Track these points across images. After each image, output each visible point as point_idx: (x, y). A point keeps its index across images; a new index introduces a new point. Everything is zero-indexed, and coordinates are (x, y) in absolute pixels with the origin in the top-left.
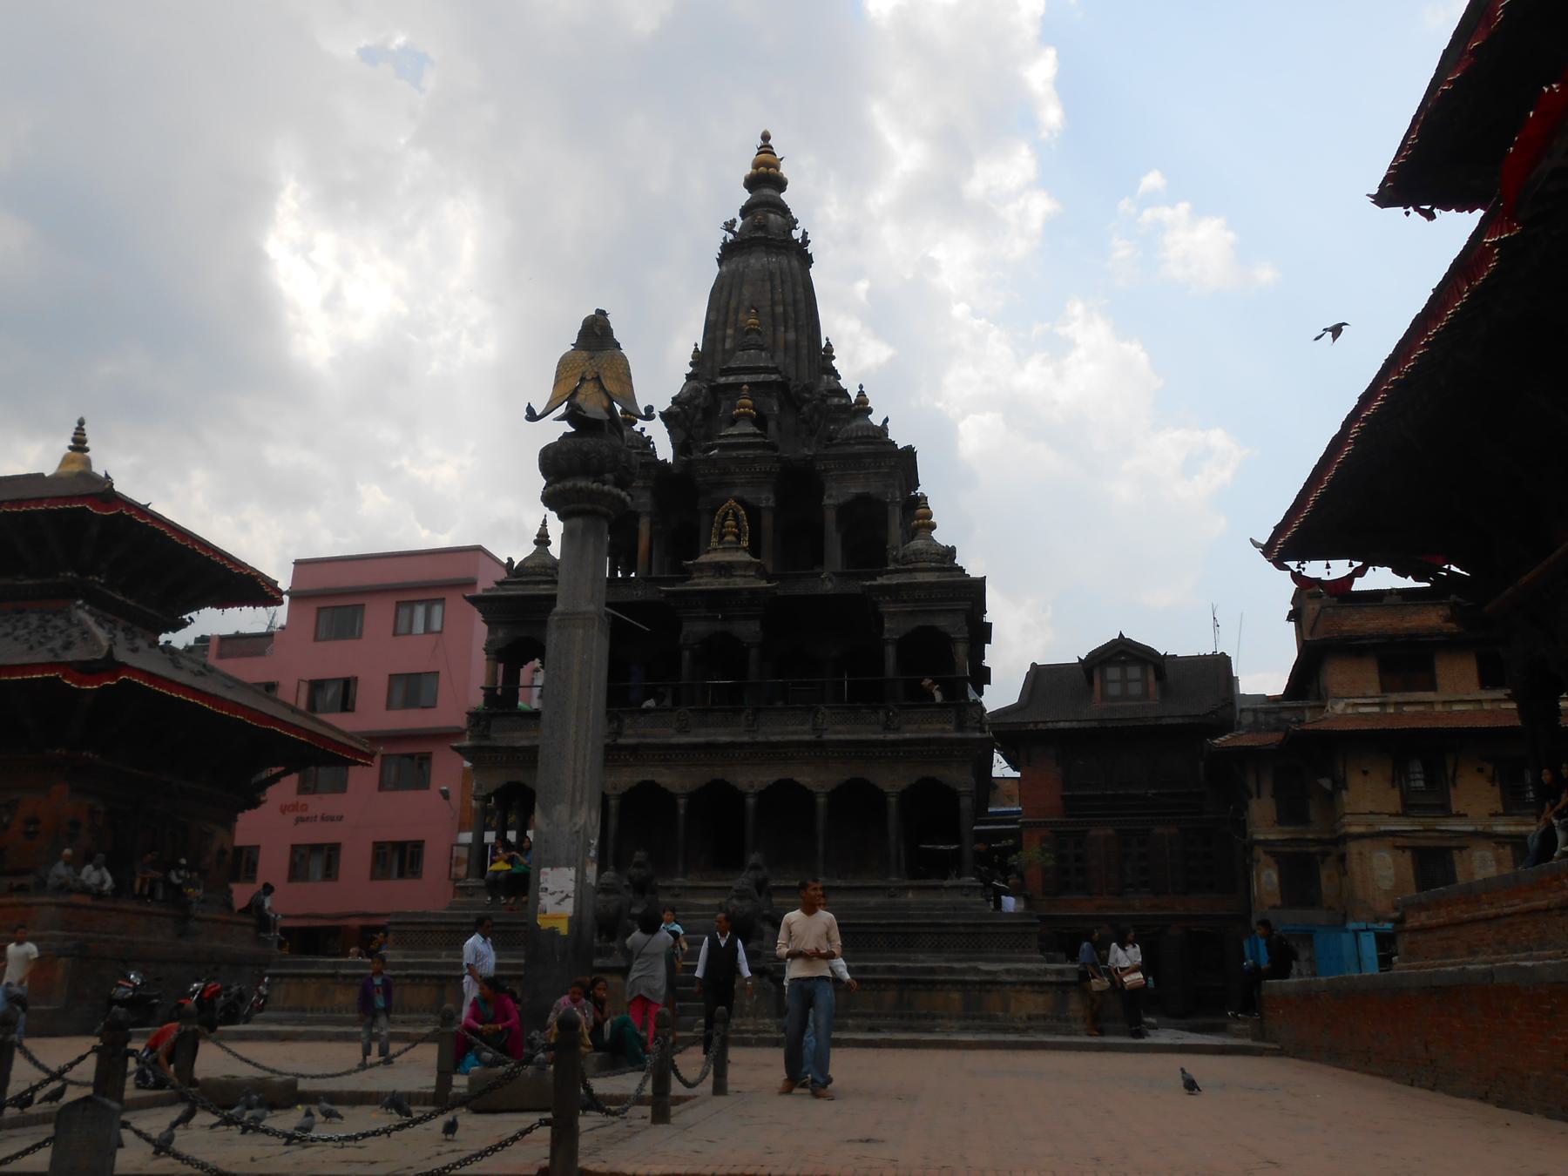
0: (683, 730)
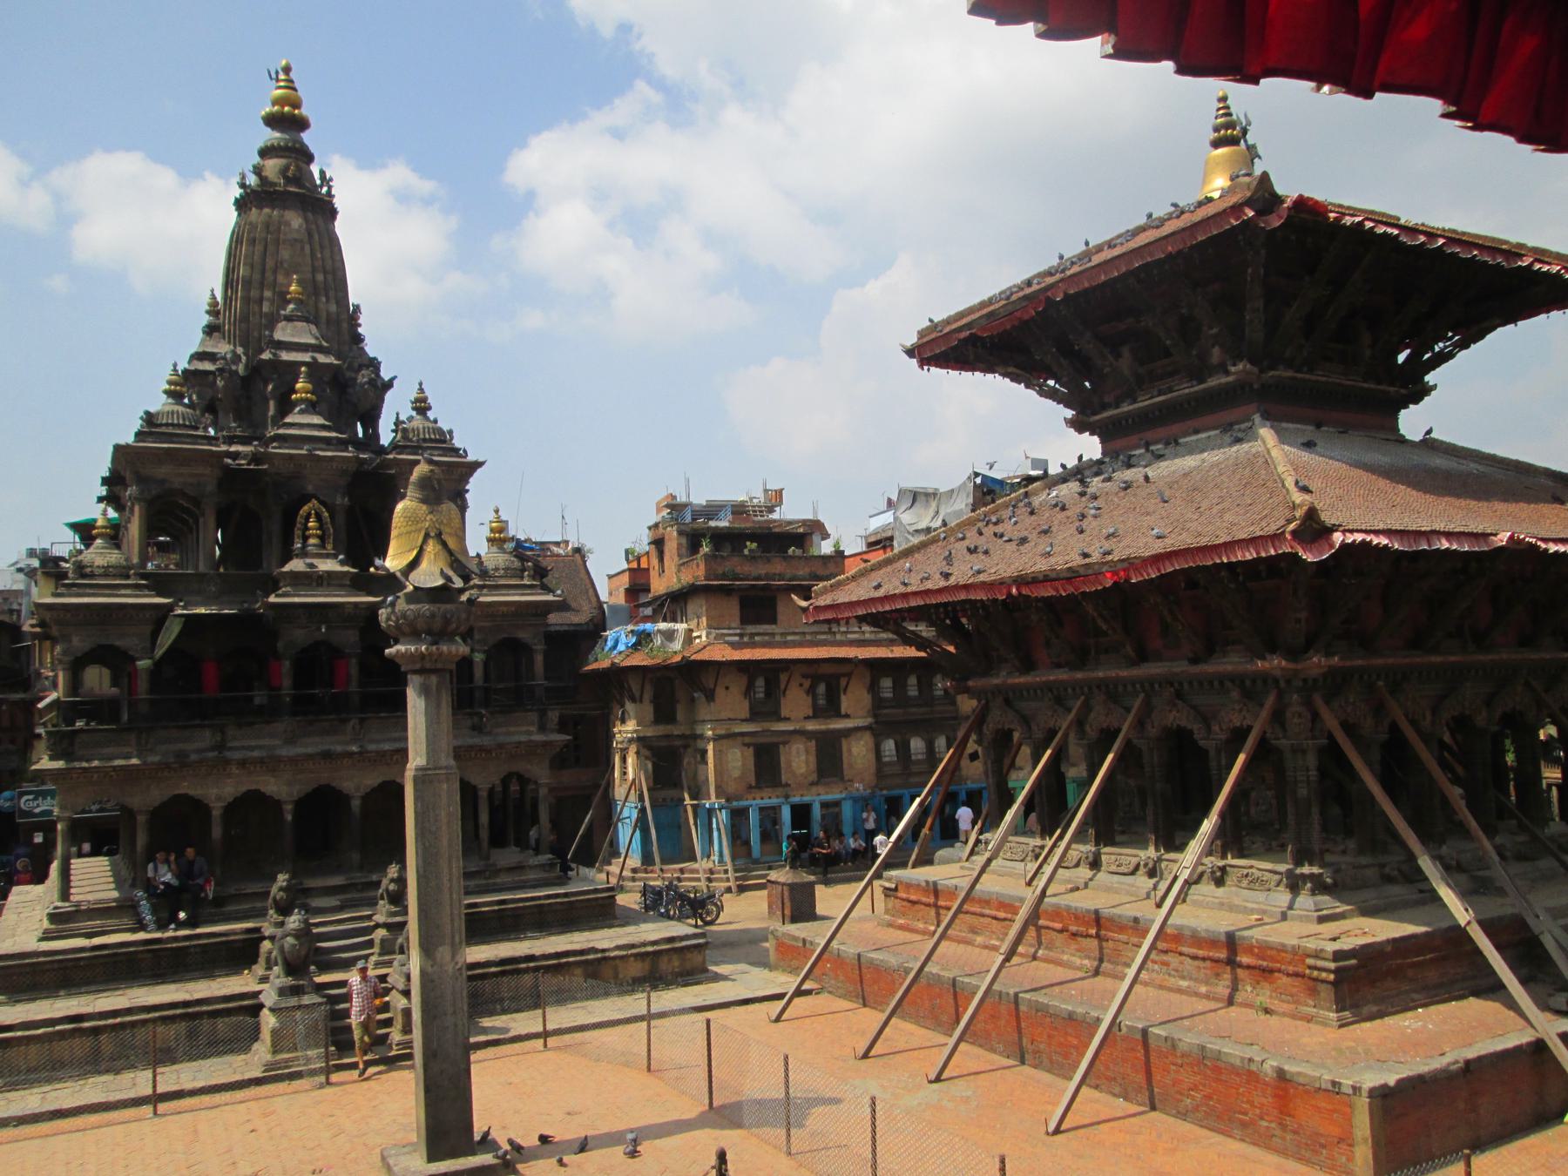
0: (291, 741)
